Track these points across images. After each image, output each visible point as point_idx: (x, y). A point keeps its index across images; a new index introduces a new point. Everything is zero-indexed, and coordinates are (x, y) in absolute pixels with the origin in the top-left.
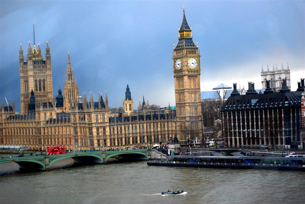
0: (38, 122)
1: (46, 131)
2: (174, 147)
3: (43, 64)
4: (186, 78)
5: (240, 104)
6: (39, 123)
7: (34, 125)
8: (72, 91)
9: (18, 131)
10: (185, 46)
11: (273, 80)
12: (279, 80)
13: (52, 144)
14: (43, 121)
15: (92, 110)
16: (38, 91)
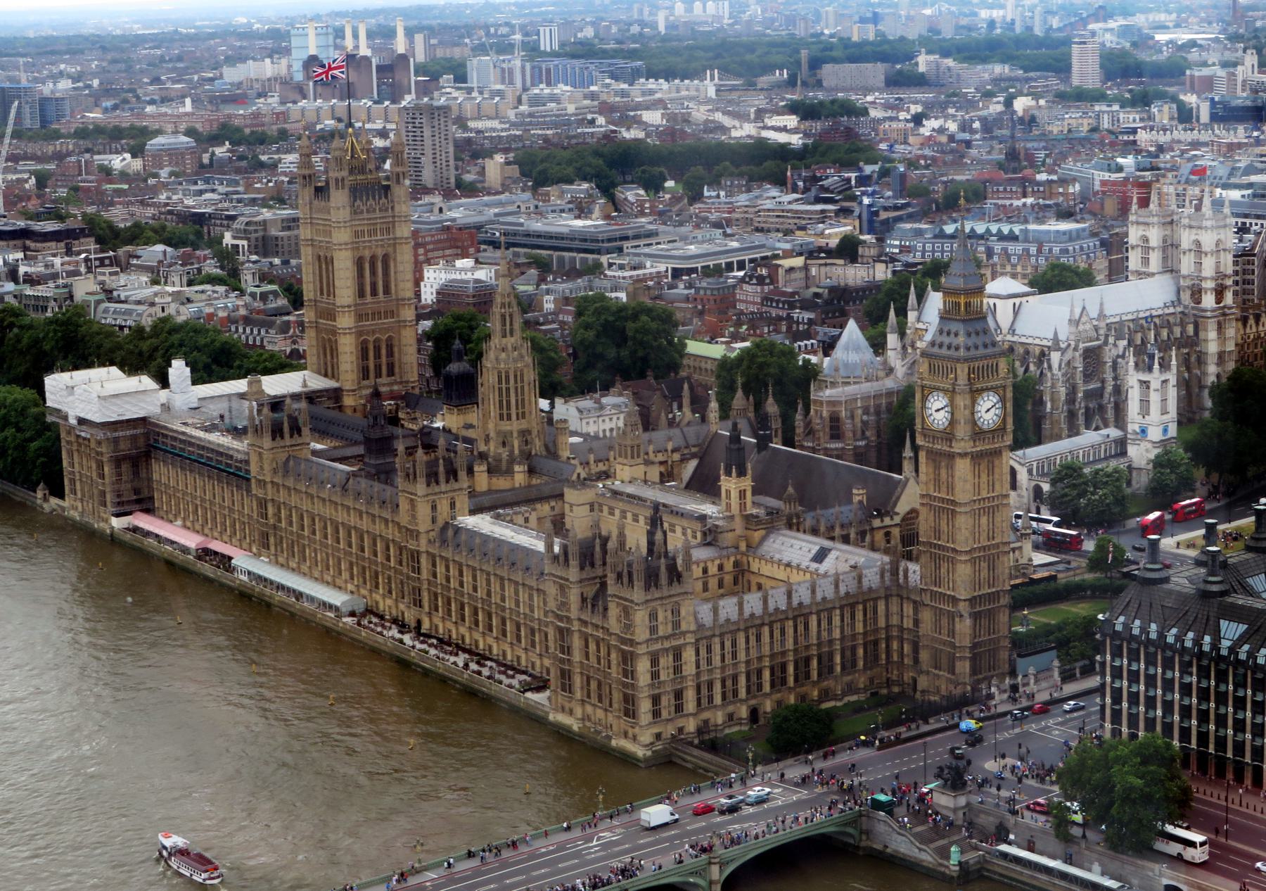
0: (412, 531)
1: (440, 569)
2: (952, 805)
3: (383, 200)
4: (963, 467)
5: (1173, 626)
6: (414, 534)
7: (391, 533)
8: (516, 376)
9: (325, 528)
10: (968, 349)
11: (1169, 242)
12: (1193, 247)
13: (463, 620)
14: (428, 532)
15: (638, 594)
16: (369, 299)
